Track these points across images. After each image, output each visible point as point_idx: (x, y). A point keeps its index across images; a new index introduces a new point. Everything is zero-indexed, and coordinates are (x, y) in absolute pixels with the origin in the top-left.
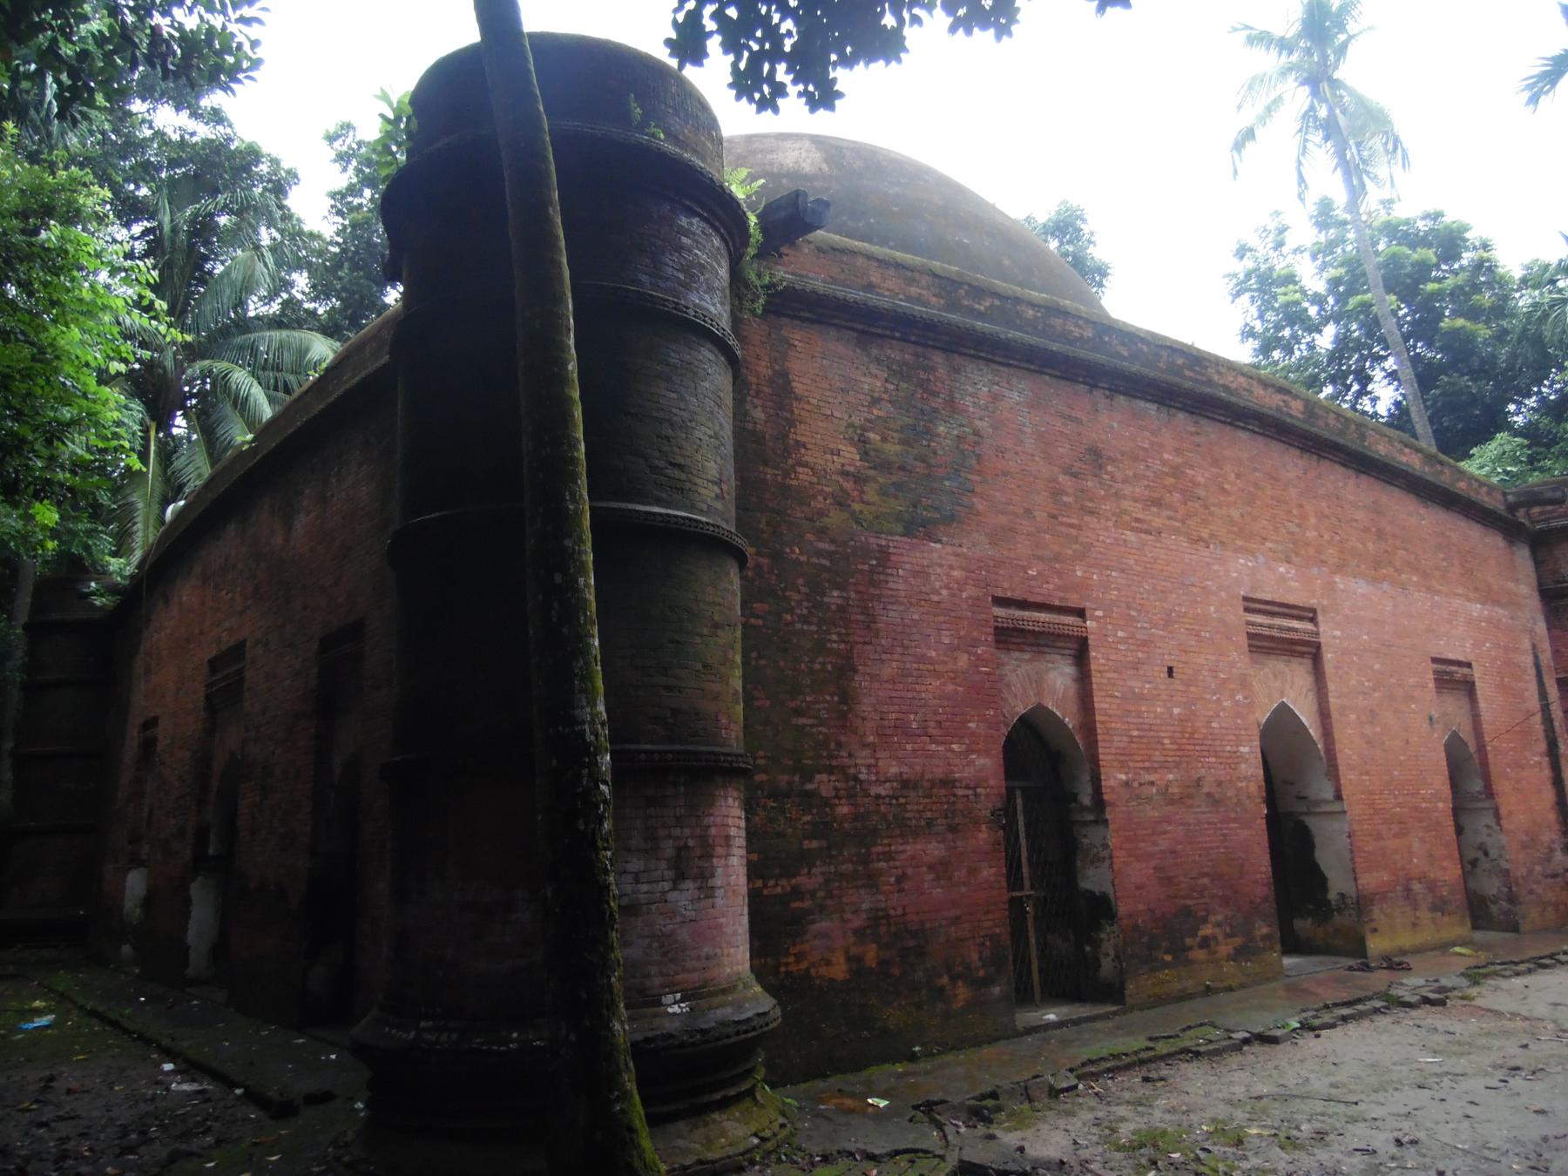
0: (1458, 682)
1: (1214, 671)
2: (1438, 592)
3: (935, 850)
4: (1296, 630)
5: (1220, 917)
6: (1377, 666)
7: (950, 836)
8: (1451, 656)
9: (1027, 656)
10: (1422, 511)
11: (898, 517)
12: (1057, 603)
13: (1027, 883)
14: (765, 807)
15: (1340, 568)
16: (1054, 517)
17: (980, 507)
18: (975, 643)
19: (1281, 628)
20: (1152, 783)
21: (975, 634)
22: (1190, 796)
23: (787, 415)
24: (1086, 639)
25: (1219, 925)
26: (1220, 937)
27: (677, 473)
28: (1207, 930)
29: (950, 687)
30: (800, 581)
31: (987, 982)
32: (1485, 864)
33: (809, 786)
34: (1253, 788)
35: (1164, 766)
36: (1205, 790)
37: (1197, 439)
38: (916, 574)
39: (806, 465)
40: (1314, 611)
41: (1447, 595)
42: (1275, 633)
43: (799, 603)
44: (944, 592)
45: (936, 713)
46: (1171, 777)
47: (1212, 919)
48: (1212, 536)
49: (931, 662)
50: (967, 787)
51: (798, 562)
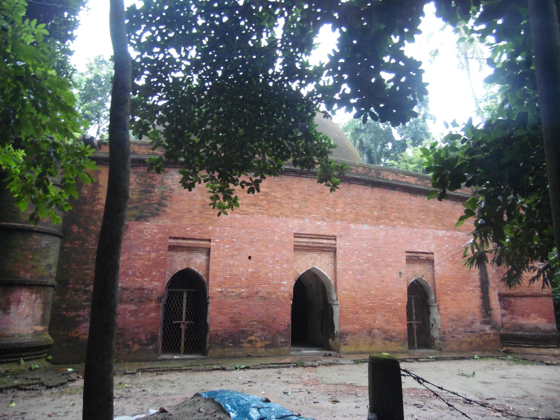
0: (424, 260)
1: (274, 257)
2: (415, 228)
3: (132, 307)
4: (323, 243)
5: (259, 335)
6: (369, 255)
7: (139, 304)
8: (419, 251)
10: (413, 198)
11: (134, 216)
12: (198, 238)
13: (184, 319)
14: (71, 294)
15: (356, 220)
16: (202, 212)
18: (159, 250)
19: (314, 243)
20: (234, 292)
21: (160, 248)
22: (253, 297)
23: (96, 191)
24: (210, 248)
25: (259, 337)
26: (258, 340)
28: (252, 338)
29: (146, 263)
30: (93, 235)
31: (148, 345)
32: (435, 326)
33: (87, 289)
34: (286, 295)
35: (241, 287)
36: (261, 294)
37: (280, 183)
38: (138, 232)
39: (101, 204)
40: (336, 237)
41: (422, 228)
42: (310, 245)
44: (149, 236)
45: (140, 269)
46: (243, 290)
47: (256, 334)
48: (281, 214)
49: (140, 255)
50: (149, 290)
51: (93, 230)
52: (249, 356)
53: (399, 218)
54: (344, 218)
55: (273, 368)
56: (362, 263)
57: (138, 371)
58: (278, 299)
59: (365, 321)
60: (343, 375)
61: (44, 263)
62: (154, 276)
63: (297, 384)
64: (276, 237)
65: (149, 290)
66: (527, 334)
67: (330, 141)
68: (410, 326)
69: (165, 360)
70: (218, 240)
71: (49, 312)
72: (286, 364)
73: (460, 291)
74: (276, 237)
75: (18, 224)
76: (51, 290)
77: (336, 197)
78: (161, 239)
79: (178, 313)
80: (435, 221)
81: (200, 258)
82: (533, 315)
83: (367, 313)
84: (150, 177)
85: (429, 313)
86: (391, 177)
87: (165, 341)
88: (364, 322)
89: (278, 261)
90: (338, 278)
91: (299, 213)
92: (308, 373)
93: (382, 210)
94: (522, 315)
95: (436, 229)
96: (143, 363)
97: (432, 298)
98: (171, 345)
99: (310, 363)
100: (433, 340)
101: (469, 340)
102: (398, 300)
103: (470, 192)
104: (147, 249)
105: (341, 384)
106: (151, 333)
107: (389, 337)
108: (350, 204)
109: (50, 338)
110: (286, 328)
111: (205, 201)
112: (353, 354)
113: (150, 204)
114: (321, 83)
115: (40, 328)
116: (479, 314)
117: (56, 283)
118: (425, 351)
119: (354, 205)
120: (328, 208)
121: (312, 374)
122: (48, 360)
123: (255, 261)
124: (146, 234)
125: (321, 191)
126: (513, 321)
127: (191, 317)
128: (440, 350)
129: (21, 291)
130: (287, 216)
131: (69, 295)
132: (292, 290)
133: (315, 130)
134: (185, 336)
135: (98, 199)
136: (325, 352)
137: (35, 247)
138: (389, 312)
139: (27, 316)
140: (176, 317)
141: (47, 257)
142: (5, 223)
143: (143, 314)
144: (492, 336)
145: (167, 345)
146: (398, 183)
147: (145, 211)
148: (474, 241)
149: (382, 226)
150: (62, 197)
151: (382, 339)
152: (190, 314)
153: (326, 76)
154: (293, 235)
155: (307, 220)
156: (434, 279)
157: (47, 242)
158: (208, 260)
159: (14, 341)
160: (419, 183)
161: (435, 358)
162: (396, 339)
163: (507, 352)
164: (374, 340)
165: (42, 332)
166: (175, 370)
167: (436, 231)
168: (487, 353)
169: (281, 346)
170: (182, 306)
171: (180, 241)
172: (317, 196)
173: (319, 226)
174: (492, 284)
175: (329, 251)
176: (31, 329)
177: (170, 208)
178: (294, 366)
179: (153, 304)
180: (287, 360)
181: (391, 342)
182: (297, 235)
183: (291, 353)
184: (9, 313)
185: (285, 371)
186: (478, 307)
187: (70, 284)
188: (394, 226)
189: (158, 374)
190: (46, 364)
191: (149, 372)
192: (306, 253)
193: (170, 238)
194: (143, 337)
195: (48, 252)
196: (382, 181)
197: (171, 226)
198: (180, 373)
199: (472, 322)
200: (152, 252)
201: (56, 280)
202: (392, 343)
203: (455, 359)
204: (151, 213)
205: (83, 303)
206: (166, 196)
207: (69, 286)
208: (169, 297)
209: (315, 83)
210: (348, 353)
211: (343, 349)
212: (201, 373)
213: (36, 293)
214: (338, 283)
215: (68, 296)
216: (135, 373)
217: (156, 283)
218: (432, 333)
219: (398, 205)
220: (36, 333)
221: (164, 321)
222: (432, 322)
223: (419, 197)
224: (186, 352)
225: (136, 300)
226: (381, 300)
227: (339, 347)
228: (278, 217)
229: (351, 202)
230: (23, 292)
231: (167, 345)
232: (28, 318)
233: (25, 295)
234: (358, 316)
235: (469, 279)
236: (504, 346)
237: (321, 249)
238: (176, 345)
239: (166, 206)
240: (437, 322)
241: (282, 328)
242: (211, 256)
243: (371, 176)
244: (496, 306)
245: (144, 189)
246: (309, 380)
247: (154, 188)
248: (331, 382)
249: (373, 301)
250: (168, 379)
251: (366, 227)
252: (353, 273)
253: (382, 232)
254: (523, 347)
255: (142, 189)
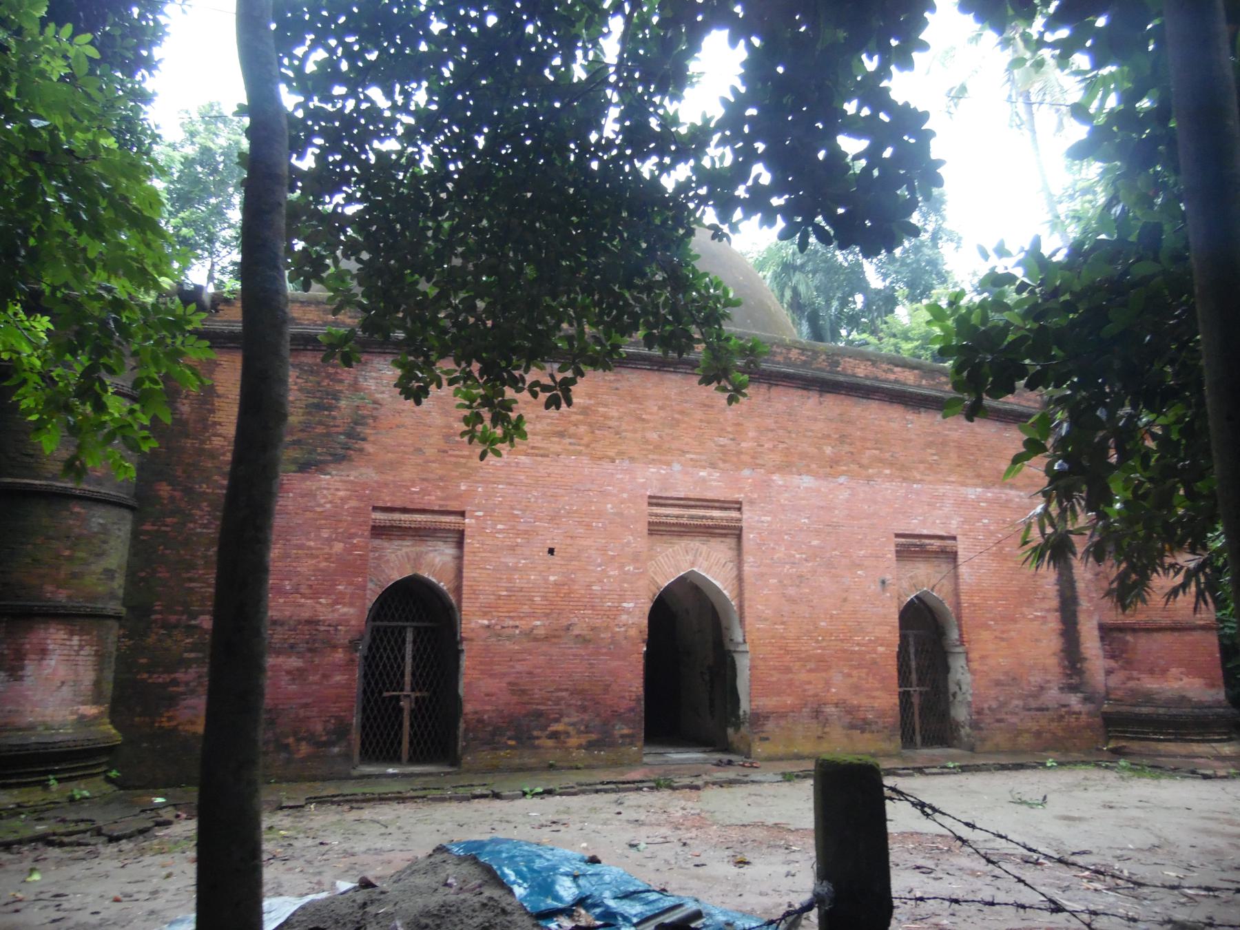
3: (294, 662)
4: (712, 518)
5: (574, 720)
6: (815, 543)
7: (309, 655)
8: (925, 532)
9: (409, 543)
11: (295, 461)
12: (436, 508)
13: (408, 688)
14: (157, 634)
15: (785, 467)
17: (371, 450)
18: (352, 536)
19: (692, 517)
21: (353, 531)
22: (559, 637)
25: (573, 724)
27: (27, 459)
29: (323, 564)
32: (959, 697)
33: (193, 622)
34: (633, 632)
35: (532, 615)
36: (576, 632)
37: (618, 385)
39: (220, 435)
40: (741, 503)
41: (930, 483)
43: (202, 517)
44: (328, 506)
45: (308, 580)
46: (538, 623)
47: (566, 720)
49: (310, 548)
50: (329, 625)
51: (204, 493)
52: (551, 766)
53: (882, 461)
54: (759, 461)
55: (606, 791)
56: (800, 559)
57: (309, 801)
58: (613, 641)
59: (807, 687)
60: (759, 805)
61: (98, 567)
62: (340, 593)
63: (659, 825)
64: (609, 506)
65: (329, 625)
66: (1161, 711)
67: (726, 292)
68: (905, 698)
69: (369, 776)
70: (480, 514)
71: (109, 675)
72: (634, 782)
73: (1014, 620)
74: (609, 506)
75: (37, 482)
76: (114, 624)
77: (741, 415)
78: (356, 512)
79: (395, 675)
80: (959, 466)
81: (442, 554)
82: (1174, 671)
83: (810, 671)
84: (328, 376)
85: (947, 669)
86: (861, 371)
87: (367, 735)
88: (805, 690)
89: (613, 557)
90: (747, 595)
91: (660, 452)
92: (683, 803)
93: (842, 442)
94: (1151, 672)
95: (963, 484)
96: (318, 784)
97: (954, 635)
98: (380, 742)
99: (687, 781)
100: (957, 726)
101: (1035, 728)
102: (880, 641)
103: (1036, 401)
104: (325, 534)
105: (755, 825)
106: (336, 718)
107: (860, 723)
108: (772, 430)
109: (114, 731)
110: (633, 704)
111: (451, 427)
112: (781, 759)
113: (328, 435)
114: (706, 163)
115: (90, 710)
116: (1058, 670)
117: (123, 611)
118: (937, 751)
119: (781, 432)
120: (722, 441)
121: (690, 804)
122: (109, 780)
123: (563, 558)
124: (322, 501)
125: (707, 402)
126: (1131, 684)
127: (424, 684)
128: (972, 749)
129: (46, 629)
130: (632, 459)
131: (154, 637)
132: (646, 622)
133: (693, 267)
134: (412, 725)
135: (215, 423)
136: (718, 756)
137: (77, 530)
138: (859, 667)
139: (63, 683)
140: (391, 683)
141: (101, 555)
142: (9, 480)
143: (317, 678)
144: (1084, 718)
145: (371, 744)
146: (877, 384)
147: (319, 450)
148: (1046, 509)
149: (842, 479)
150: (135, 419)
151: (844, 728)
152: (421, 675)
153: (717, 146)
154: (646, 500)
155: (677, 467)
156: (956, 593)
157: (101, 521)
158: (460, 558)
159: (33, 739)
160: (924, 382)
161: (960, 767)
162: (874, 727)
163: (1118, 753)
164: (827, 730)
165: (95, 717)
166: (390, 799)
167: (963, 490)
168: (1075, 755)
169: (623, 744)
170: (403, 658)
171: (397, 516)
172: (699, 414)
173: (704, 480)
174: (1084, 604)
175: (725, 535)
176: (72, 713)
177: (374, 443)
178: (651, 788)
179: (339, 655)
180: (635, 775)
181: (863, 731)
182: (654, 501)
183: (645, 759)
184: (21, 678)
185: (632, 798)
186: (1054, 654)
187: (156, 612)
188: (869, 479)
189: (352, 808)
190: (108, 788)
191: (333, 803)
192: (675, 540)
193: (375, 509)
194: (319, 728)
195: (105, 542)
196: (841, 379)
197: (376, 482)
198: (402, 806)
199: (1042, 688)
200: (336, 540)
201: (124, 605)
202: (867, 736)
203: (1003, 768)
204: (331, 455)
205: (186, 655)
206: (364, 417)
207: (153, 617)
208: (374, 639)
209: (692, 162)
210: (770, 759)
211: (759, 749)
212: (446, 804)
213: (81, 632)
214: (746, 604)
215: (151, 640)
216: (302, 806)
217: (345, 610)
218: (953, 713)
219: (877, 433)
220: (82, 720)
221: (365, 692)
222: (953, 688)
223: (923, 415)
224: (413, 760)
225: (302, 647)
226: (842, 641)
227: (749, 746)
228: (613, 461)
229: (773, 426)
230: (52, 630)
231: (371, 744)
232: (64, 688)
233: (56, 637)
234: (790, 676)
235: (1036, 593)
236: (1110, 738)
237: (709, 531)
238: (392, 743)
239: (364, 439)
240: (964, 687)
241: (623, 705)
242: (466, 549)
243: (818, 369)
244: (1094, 652)
245: (315, 401)
246: (685, 817)
247: (337, 399)
248: (734, 821)
249: (824, 644)
250: (376, 817)
251: (807, 481)
252: (780, 582)
253: (841, 491)
254: (1154, 740)
255: (311, 401)
